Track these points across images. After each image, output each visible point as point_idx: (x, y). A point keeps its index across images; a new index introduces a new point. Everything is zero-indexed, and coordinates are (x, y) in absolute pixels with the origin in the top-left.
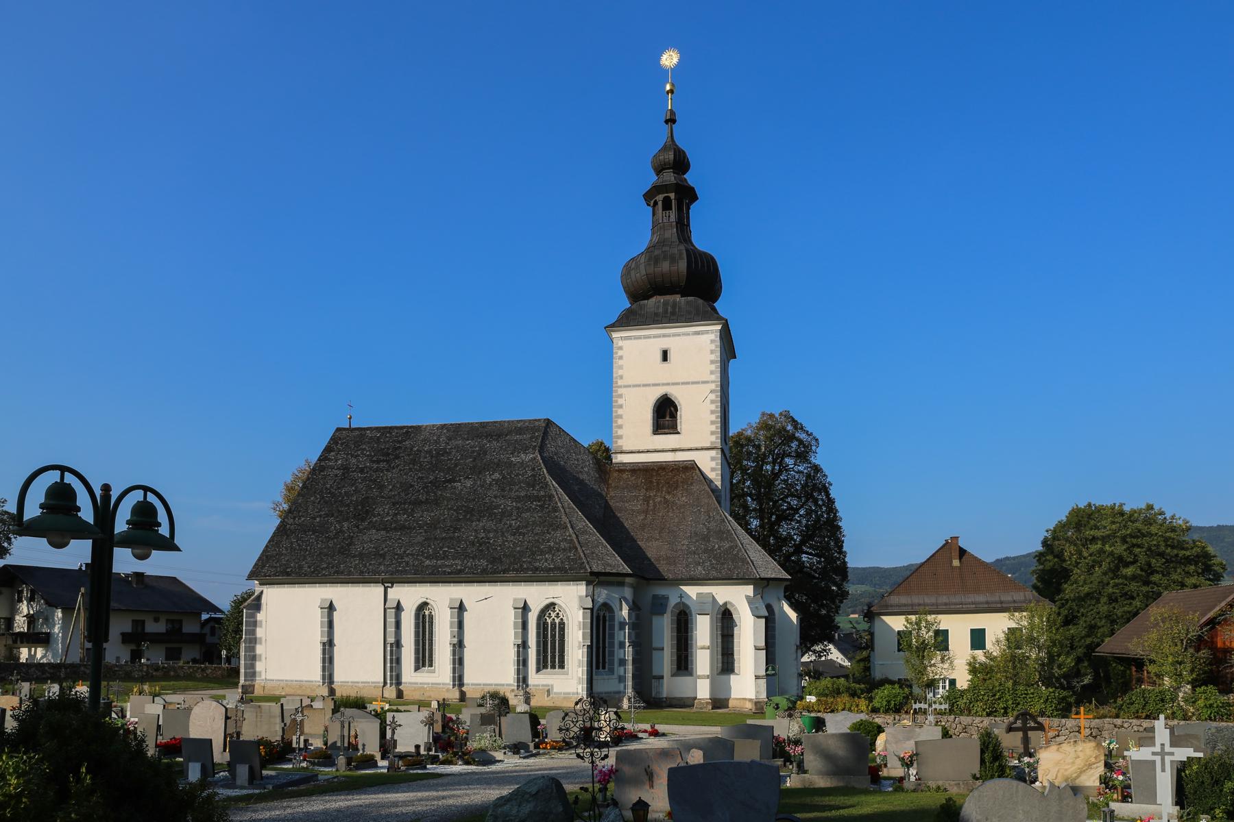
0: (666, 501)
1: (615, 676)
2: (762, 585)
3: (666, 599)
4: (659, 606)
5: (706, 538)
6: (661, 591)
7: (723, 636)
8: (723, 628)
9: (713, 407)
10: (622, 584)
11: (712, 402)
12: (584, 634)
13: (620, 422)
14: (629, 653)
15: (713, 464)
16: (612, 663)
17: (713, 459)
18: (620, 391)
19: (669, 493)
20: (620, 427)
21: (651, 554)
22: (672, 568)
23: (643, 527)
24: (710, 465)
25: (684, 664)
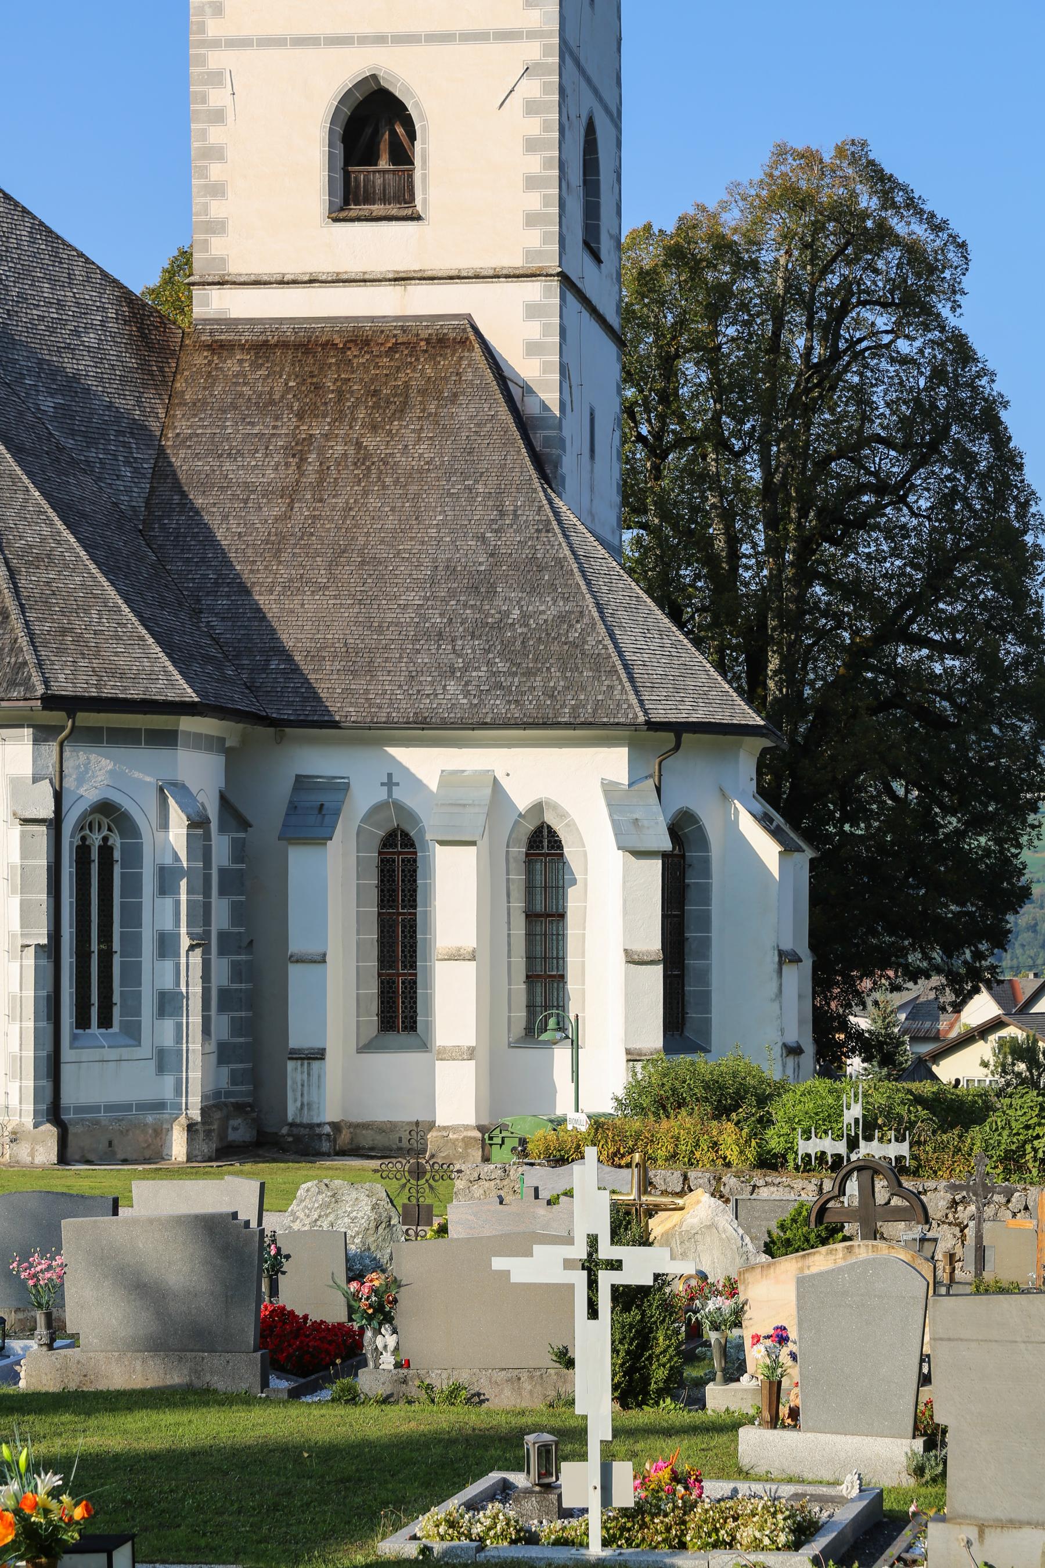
0: (363, 457)
1: (146, 1050)
2: (664, 739)
3: (341, 788)
4: (312, 812)
5: (482, 587)
6: (320, 761)
7: (531, 916)
8: (530, 888)
9: (534, 127)
10: (167, 739)
11: (531, 108)
12: (25, 909)
13: (216, 171)
14: (189, 973)
15: (534, 330)
16: (133, 1008)
17: (532, 311)
18: (216, 60)
19: (374, 428)
20: (218, 190)
21: (288, 639)
22: (359, 684)
23: (276, 545)
24: (523, 330)
25: (398, 1010)
